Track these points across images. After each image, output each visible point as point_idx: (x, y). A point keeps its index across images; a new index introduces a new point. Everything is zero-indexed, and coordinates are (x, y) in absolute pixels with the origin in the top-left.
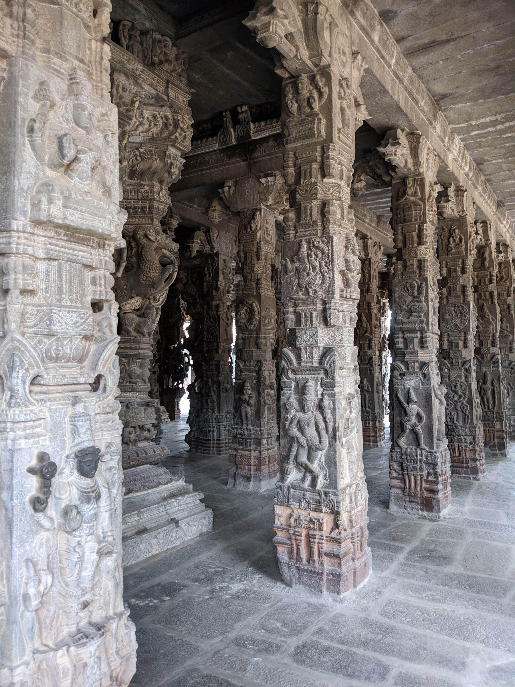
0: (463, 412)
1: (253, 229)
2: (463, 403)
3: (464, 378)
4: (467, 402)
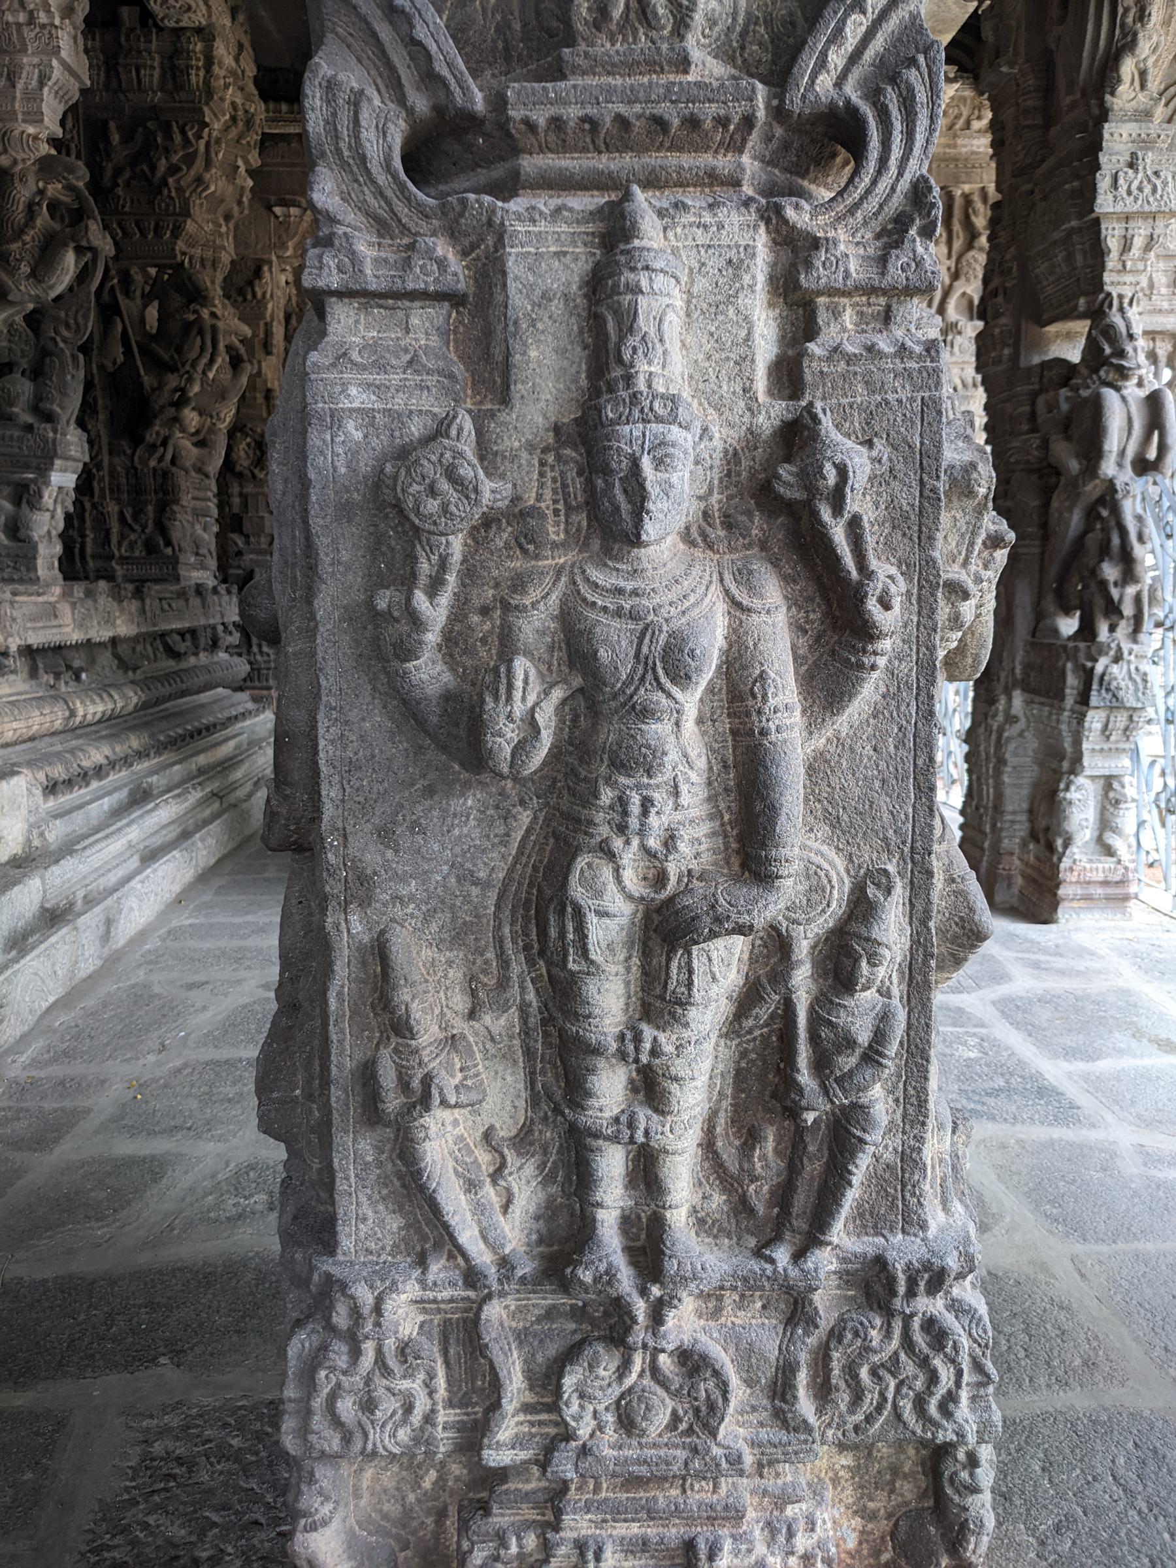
1: (259, 295)
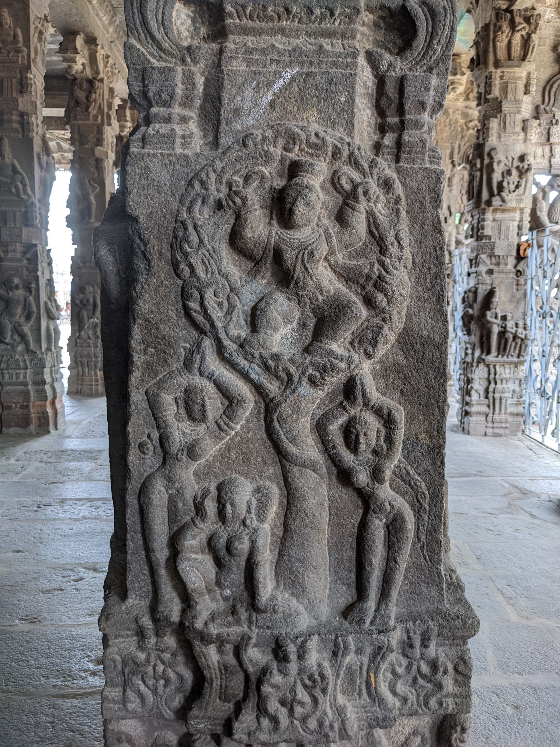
0: (344, 476)
2: (350, 389)
3: (365, 115)
4: (386, 372)
